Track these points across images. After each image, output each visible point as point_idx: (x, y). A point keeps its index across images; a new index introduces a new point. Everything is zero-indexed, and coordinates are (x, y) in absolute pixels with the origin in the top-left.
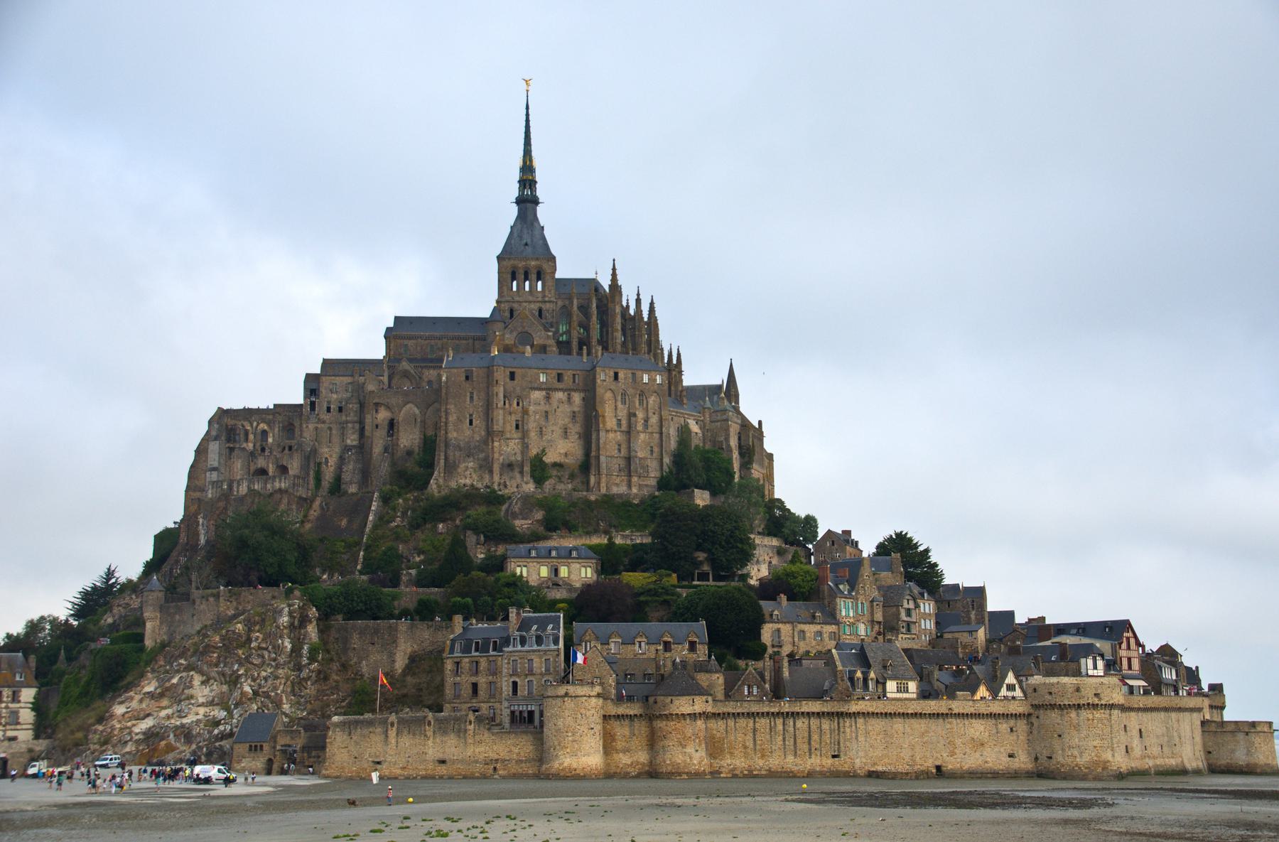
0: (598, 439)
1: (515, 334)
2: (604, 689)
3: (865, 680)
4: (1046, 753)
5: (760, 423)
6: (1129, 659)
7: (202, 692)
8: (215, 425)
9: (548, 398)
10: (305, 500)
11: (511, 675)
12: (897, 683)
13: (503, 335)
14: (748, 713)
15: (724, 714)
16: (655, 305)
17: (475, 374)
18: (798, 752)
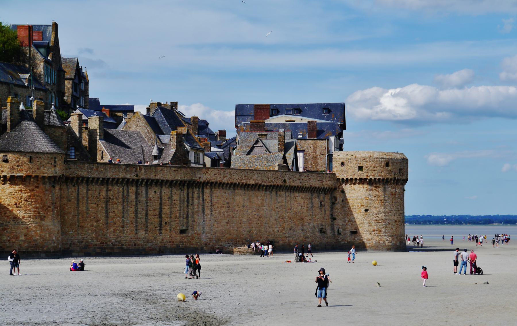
4: (350, 228)
12: (194, 152)
15: (78, 178)
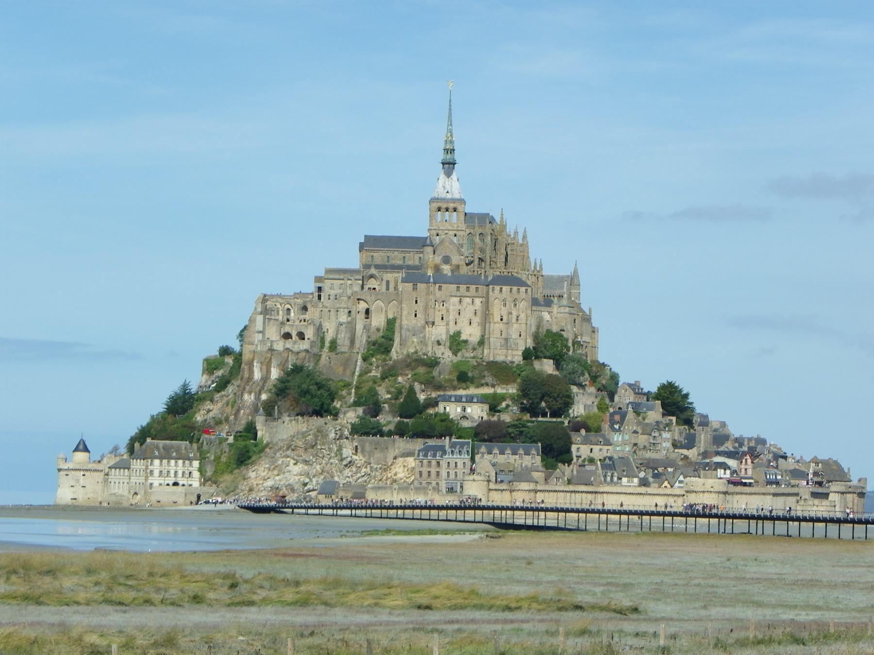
0: (490, 328)
1: (441, 257)
3: (612, 476)
6: (746, 469)
7: (297, 469)
9: (460, 302)
13: (434, 257)
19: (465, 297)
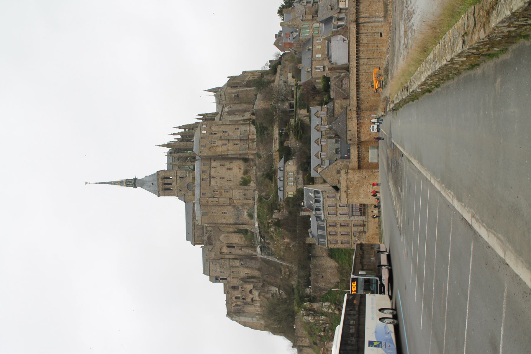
0: (232, 154)
2: (343, 169)
5: (228, 77)
8: (233, 318)
9: (214, 178)
10: (263, 284)
11: (337, 216)
12: (340, 2)
13: (189, 196)
14: (357, 86)
15: (357, 100)
16: (177, 126)
17: (204, 211)
18: (379, 56)
19: (210, 174)
